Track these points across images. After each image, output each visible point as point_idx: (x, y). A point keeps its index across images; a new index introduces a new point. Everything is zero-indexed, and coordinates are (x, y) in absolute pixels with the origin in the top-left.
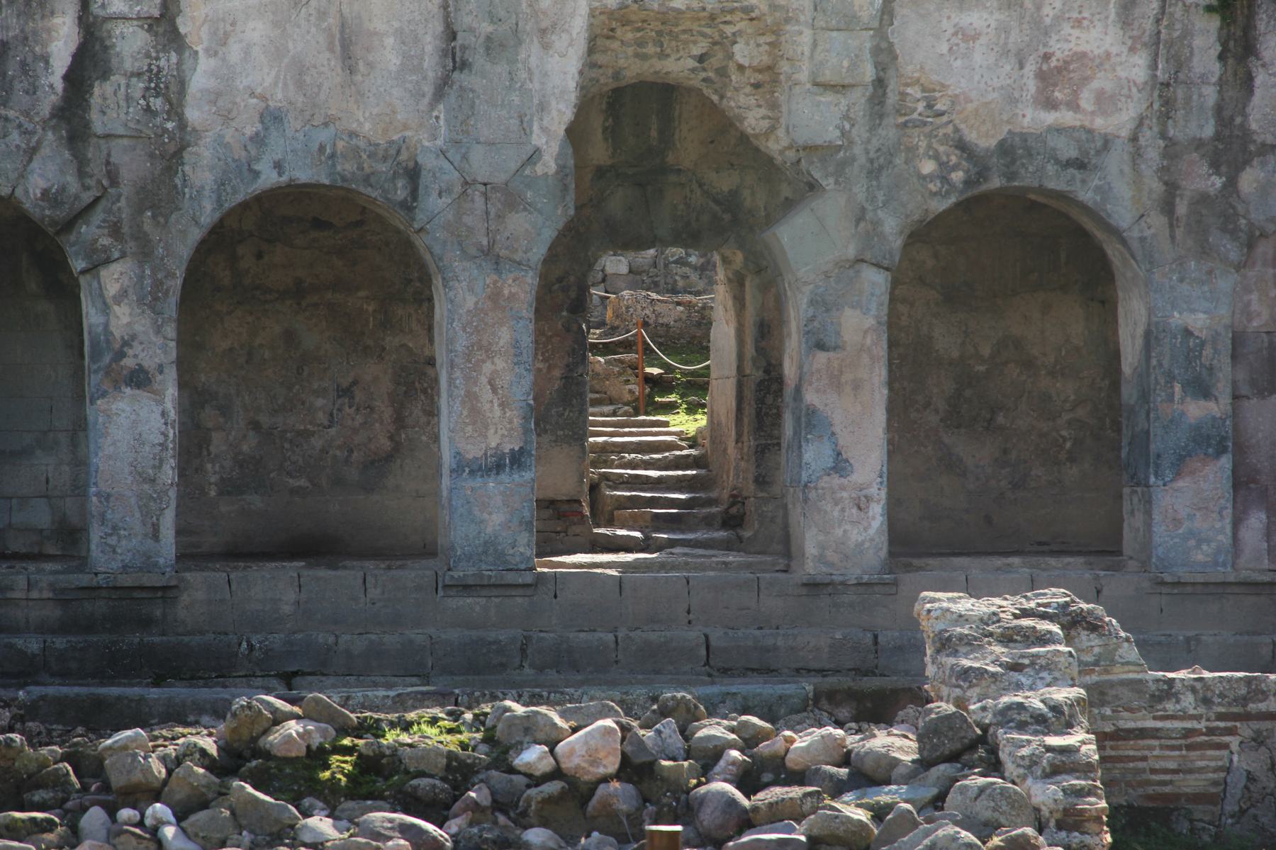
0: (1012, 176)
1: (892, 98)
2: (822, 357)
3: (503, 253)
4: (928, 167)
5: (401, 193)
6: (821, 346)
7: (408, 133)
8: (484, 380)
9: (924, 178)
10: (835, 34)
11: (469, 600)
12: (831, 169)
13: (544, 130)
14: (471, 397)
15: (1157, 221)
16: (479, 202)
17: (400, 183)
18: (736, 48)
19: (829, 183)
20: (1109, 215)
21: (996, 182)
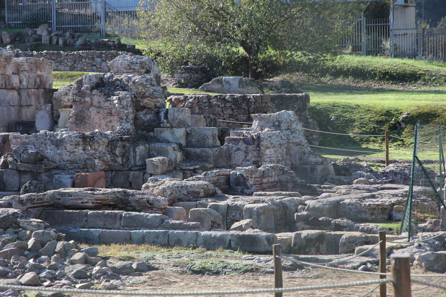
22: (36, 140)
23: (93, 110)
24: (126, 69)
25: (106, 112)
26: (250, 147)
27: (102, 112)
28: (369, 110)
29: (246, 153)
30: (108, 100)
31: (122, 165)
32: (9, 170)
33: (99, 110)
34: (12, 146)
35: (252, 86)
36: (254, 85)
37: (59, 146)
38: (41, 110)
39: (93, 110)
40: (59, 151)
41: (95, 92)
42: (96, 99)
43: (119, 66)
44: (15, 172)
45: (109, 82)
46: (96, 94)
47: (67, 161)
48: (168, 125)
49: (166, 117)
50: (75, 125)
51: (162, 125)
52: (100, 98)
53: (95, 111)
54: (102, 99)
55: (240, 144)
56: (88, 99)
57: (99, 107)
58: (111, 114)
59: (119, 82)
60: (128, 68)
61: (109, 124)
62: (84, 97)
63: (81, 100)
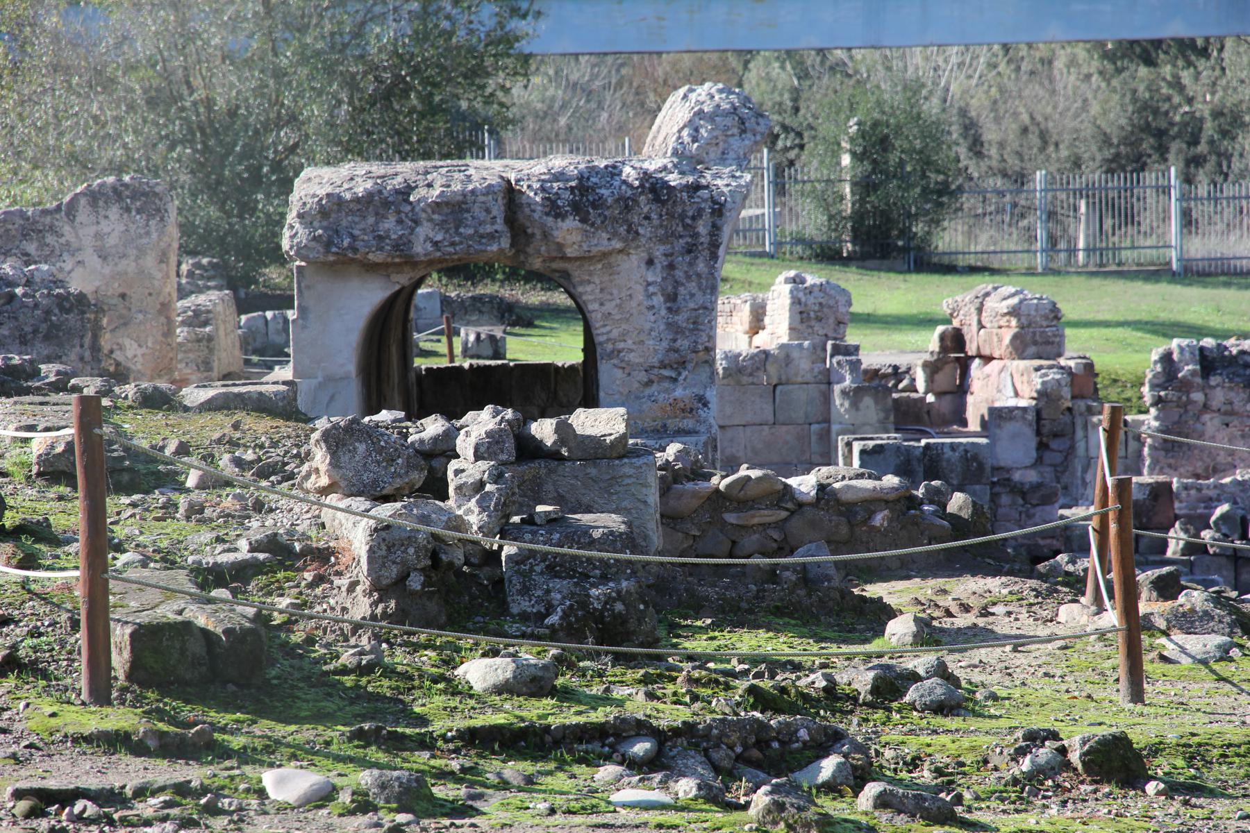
22: (1242, 491)
23: (1211, 419)
24: (1047, 318)
27: (1236, 422)
28: (1115, 381)
32: (1207, 558)
33: (1227, 419)
34: (1177, 505)
35: (481, 312)
36: (484, 309)
38: (1011, 419)
39: (1211, 419)
41: (1214, 380)
42: (1219, 397)
43: (1033, 313)
44: (1223, 561)
45: (1224, 357)
46: (1218, 385)
50: (1163, 453)
52: (1232, 395)
56: (1198, 396)
57: (1232, 413)
60: (1052, 316)
62: (1188, 393)
63: (1180, 398)
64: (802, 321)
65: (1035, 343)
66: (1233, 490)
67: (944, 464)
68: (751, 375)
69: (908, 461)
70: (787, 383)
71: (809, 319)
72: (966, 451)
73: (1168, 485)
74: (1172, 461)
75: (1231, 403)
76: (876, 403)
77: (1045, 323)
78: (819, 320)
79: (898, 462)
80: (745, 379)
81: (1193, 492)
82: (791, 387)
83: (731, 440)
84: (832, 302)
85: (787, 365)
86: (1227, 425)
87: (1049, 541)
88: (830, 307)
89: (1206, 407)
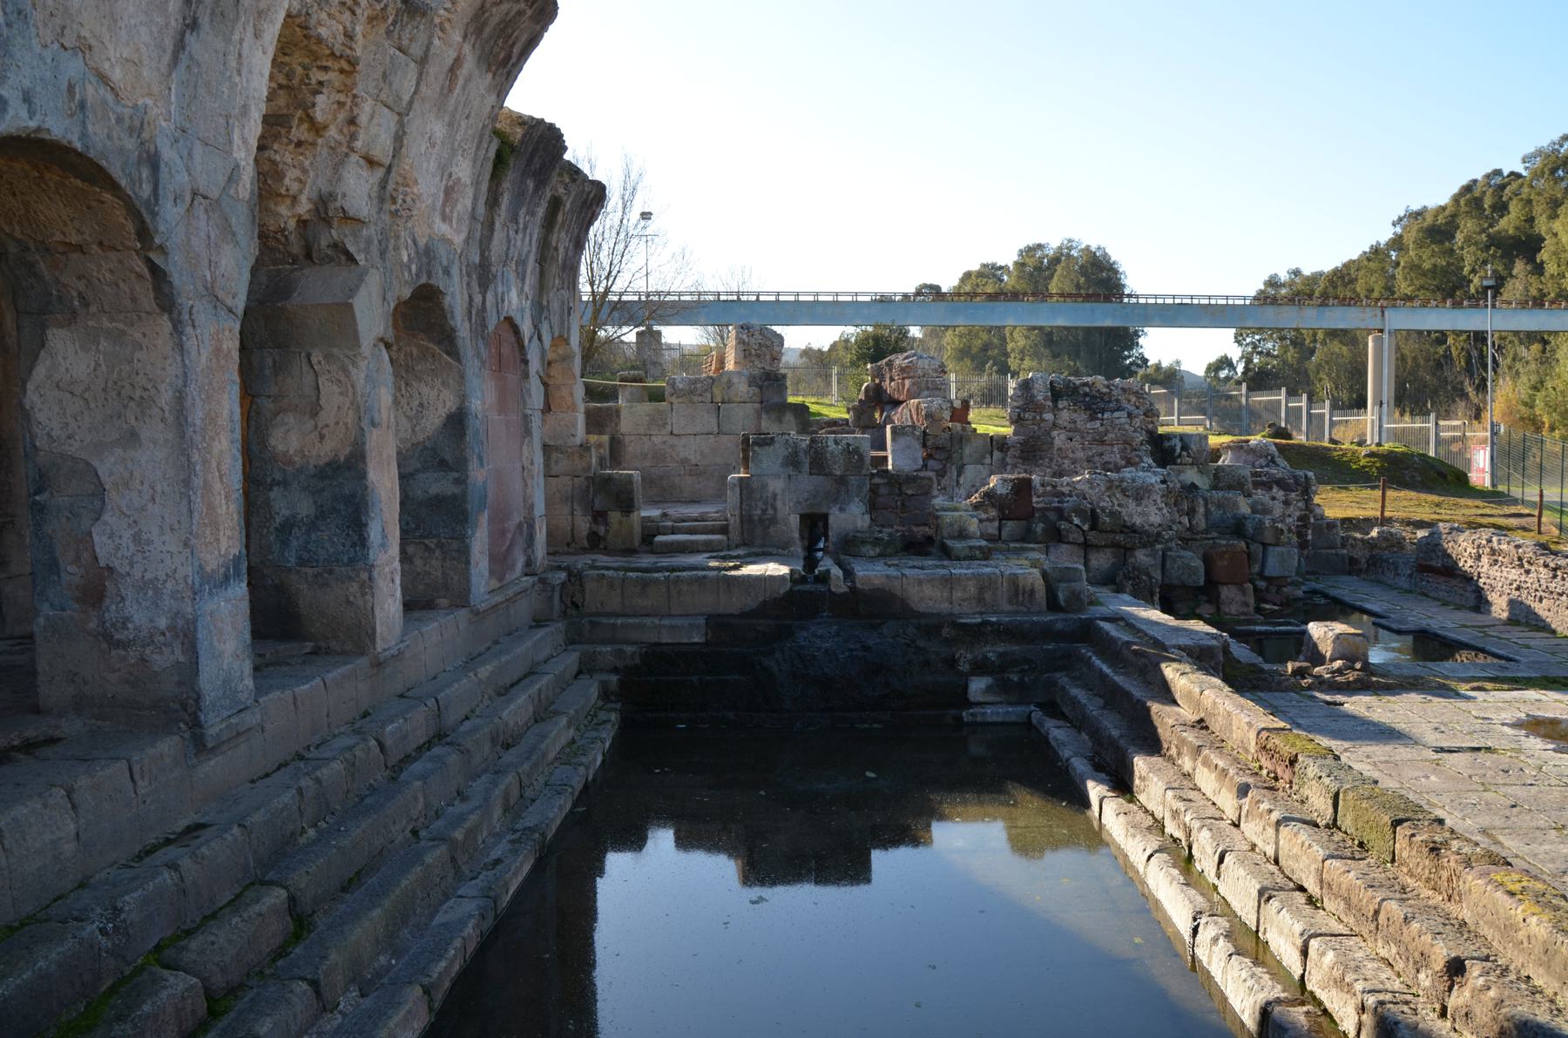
0: (429, 277)
1: (390, 187)
2: (375, 432)
3: (221, 294)
4: (405, 259)
5: (146, 190)
6: (373, 424)
7: (149, 102)
8: (214, 464)
9: (402, 265)
10: (386, 110)
11: (212, 763)
12: (362, 245)
13: (245, 141)
14: (207, 486)
15: (467, 325)
16: (203, 216)
17: (145, 173)
18: (321, 100)
19: (360, 257)
20: (453, 317)
21: (423, 280)
22: (1091, 488)
23: (1059, 435)
24: (936, 370)
25: (1089, 438)
26: (1293, 495)
29: (1287, 503)
30: (1097, 419)
31: (1188, 529)
34: (1035, 499)
37: (1142, 499)
39: (1059, 435)
40: (1139, 509)
41: (1061, 404)
42: (1065, 415)
47: (1160, 525)
48: (1190, 460)
49: (1185, 448)
51: (1179, 461)
52: (1075, 415)
53: (1063, 437)
54: (1081, 417)
55: (1275, 490)
56: (1049, 416)
57: (1076, 430)
58: (1102, 442)
59: (1087, 389)
61: (1097, 459)
62: (1041, 414)
63: (1035, 418)
64: (745, 357)
65: (928, 389)
66: (1083, 487)
67: (828, 455)
68: (701, 395)
69: (795, 453)
70: (729, 402)
71: (750, 354)
72: (848, 445)
73: (1029, 481)
74: (1028, 467)
75: (1075, 422)
76: (796, 418)
77: (935, 375)
78: (758, 356)
79: (786, 453)
80: (696, 398)
81: (1049, 488)
82: (732, 405)
83: (685, 446)
84: (768, 343)
85: (729, 388)
86: (1071, 440)
87: (921, 528)
88: (767, 347)
89: (1055, 426)
